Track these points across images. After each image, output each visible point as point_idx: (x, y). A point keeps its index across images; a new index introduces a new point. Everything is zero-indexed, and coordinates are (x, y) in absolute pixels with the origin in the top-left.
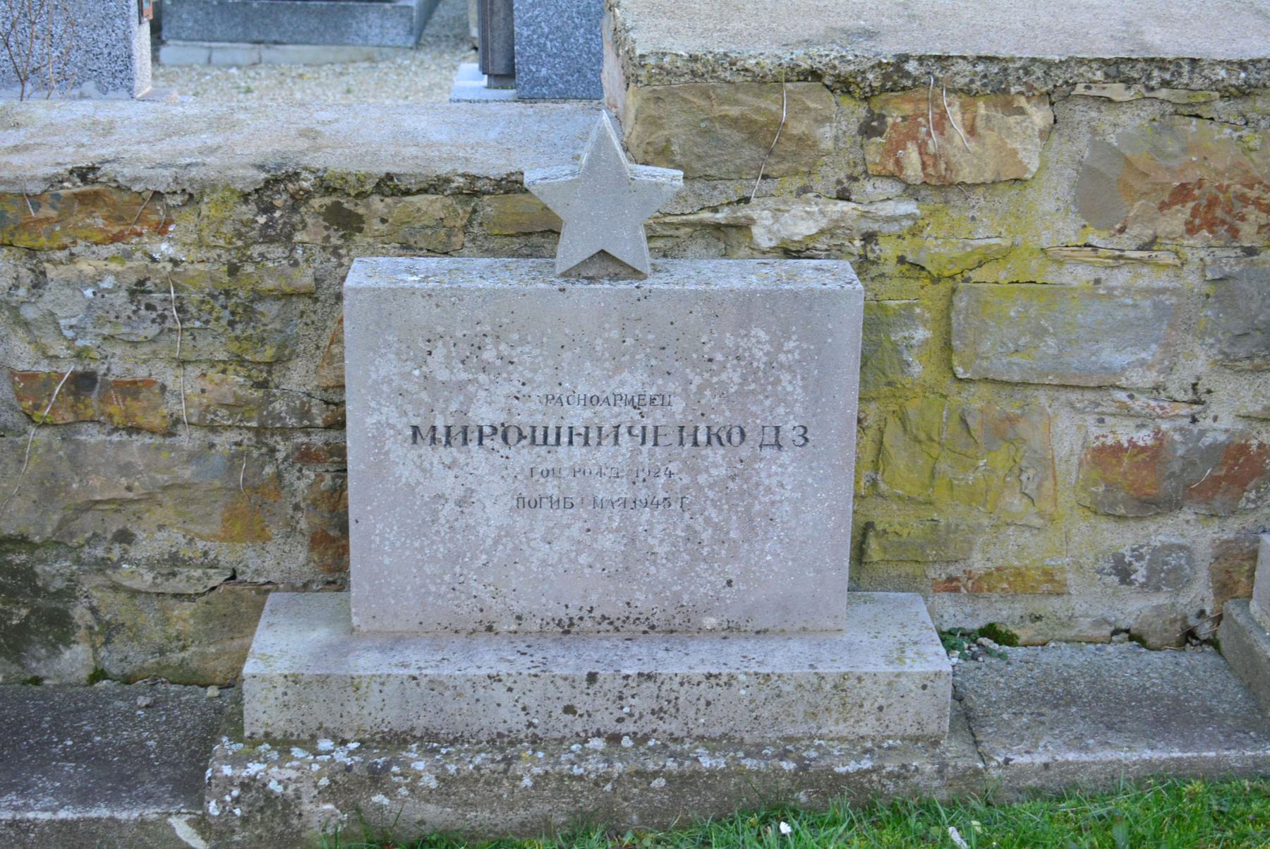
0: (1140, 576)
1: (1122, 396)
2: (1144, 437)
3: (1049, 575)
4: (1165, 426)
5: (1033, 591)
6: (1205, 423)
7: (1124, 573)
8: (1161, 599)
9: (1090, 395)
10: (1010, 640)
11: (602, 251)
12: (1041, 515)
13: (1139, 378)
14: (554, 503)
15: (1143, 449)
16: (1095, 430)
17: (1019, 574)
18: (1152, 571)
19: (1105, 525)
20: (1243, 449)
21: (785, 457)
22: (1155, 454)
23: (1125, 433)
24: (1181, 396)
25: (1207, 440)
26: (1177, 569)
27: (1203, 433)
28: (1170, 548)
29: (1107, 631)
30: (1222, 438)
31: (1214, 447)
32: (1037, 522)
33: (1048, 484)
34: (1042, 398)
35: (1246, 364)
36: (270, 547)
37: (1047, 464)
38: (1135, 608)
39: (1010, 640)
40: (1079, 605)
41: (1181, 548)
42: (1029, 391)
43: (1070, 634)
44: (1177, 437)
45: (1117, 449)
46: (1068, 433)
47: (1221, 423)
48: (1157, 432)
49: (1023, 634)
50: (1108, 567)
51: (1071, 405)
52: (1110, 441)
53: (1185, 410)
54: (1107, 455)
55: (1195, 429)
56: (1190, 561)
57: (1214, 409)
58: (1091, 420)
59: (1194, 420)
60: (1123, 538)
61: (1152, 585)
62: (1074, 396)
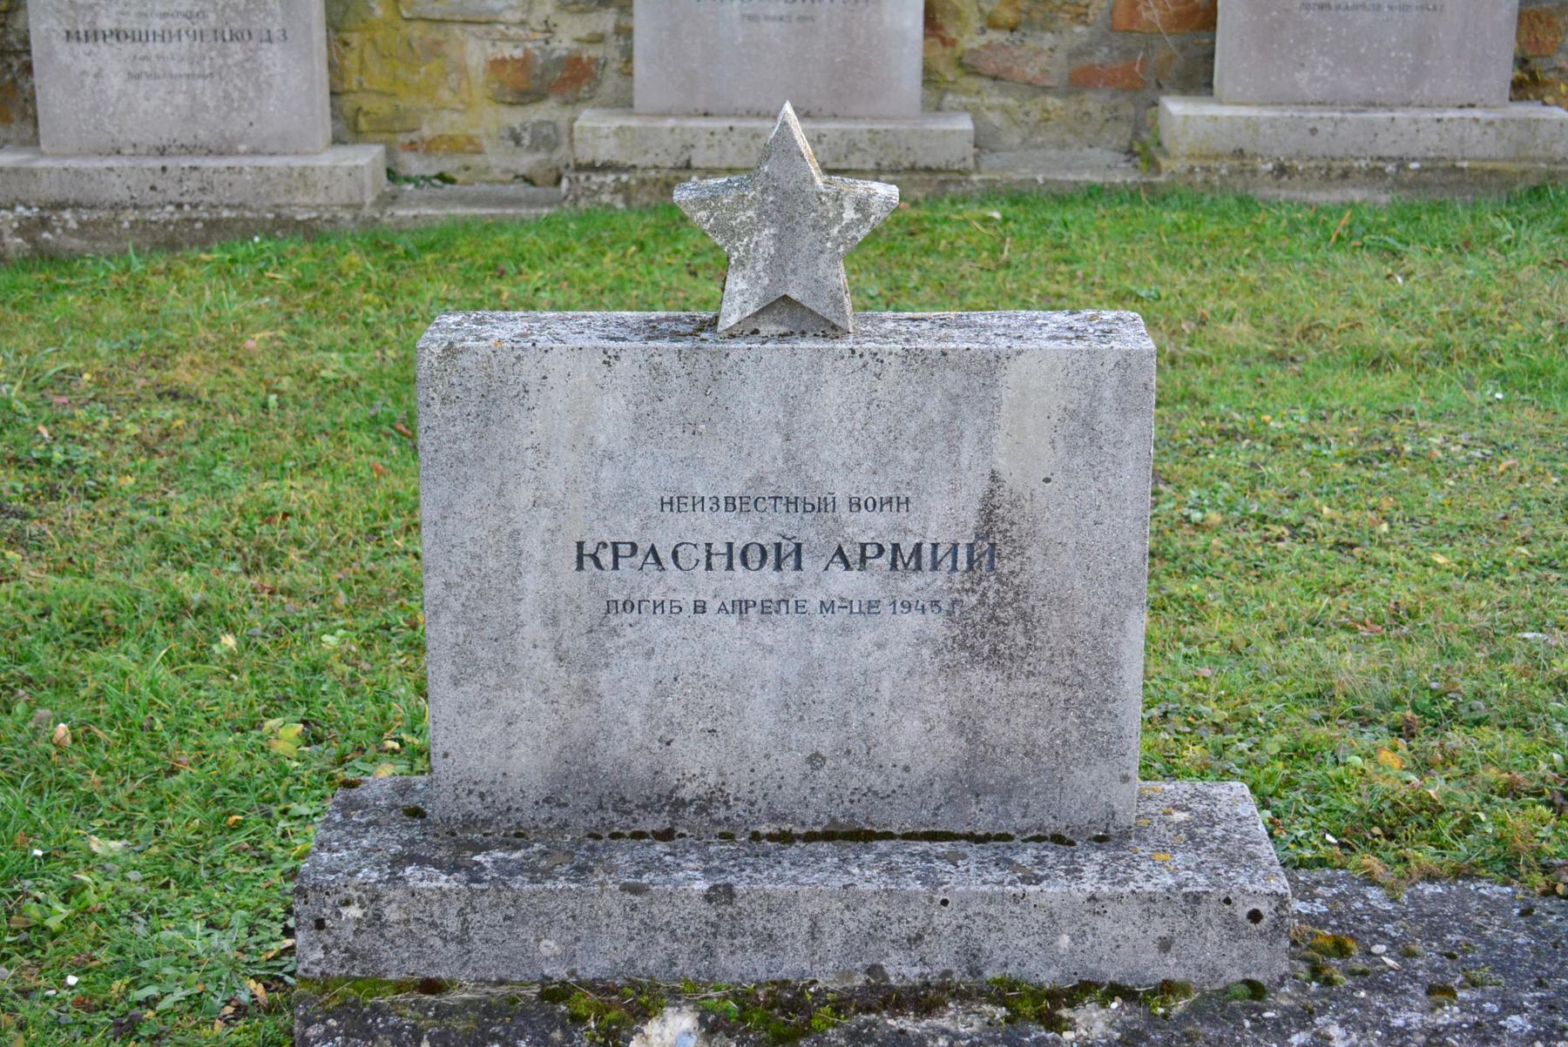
0: (526, 141)
1: (502, 27)
2: (518, 53)
3: (470, 140)
4: (529, 45)
5: (462, 151)
6: (554, 44)
7: (517, 139)
8: (541, 156)
9: (484, 28)
10: (452, 181)
11: (785, 297)
12: (462, 102)
13: (510, 16)
14: (148, 76)
15: (517, 61)
16: (490, 50)
17: (452, 139)
18: (533, 138)
19: (504, 109)
20: (578, 60)
21: (275, 47)
22: (524, 63)
23: (510, 51)
24: (539, 28)
25: (556, 54)
26: (546, 137)
27: (553, 50)
28: (541, 123)
29: (510, 176)
30: (564, 53)
31: (559, 59)
32: (461, 107)
33: (464, 83)
34: (456, 30)
35: (574, 8)
36: (14, 126)
37: (463, 70)
38: (526, 161)
39: (452, 181)
40: (493, 160)
41: (549, 123)
42: (449, 26)
43: (489, 178)
44: (537, 53)
45: (503, 61)
46: (476, 52)
47: (563, 44)
48: (526, 51)
49: (460, 177)
50: (506, 134)
51: (473, 34)
52: (499, 56)
53: (539, 36)
54: (497, 65)
55: (548, 48)
56: (556, 130)
57: (559, 35)
58: (488, 44)
59: (547, 42)
60: (515, 117)
61: (534, 148)
62: (475, 28)
